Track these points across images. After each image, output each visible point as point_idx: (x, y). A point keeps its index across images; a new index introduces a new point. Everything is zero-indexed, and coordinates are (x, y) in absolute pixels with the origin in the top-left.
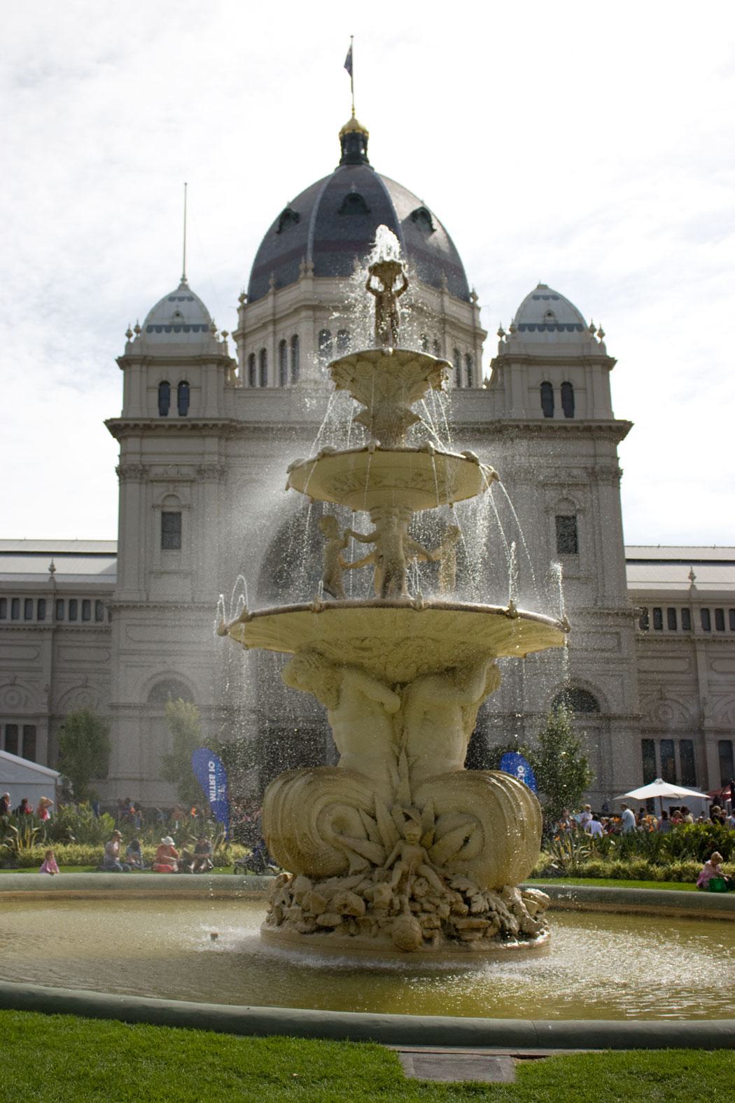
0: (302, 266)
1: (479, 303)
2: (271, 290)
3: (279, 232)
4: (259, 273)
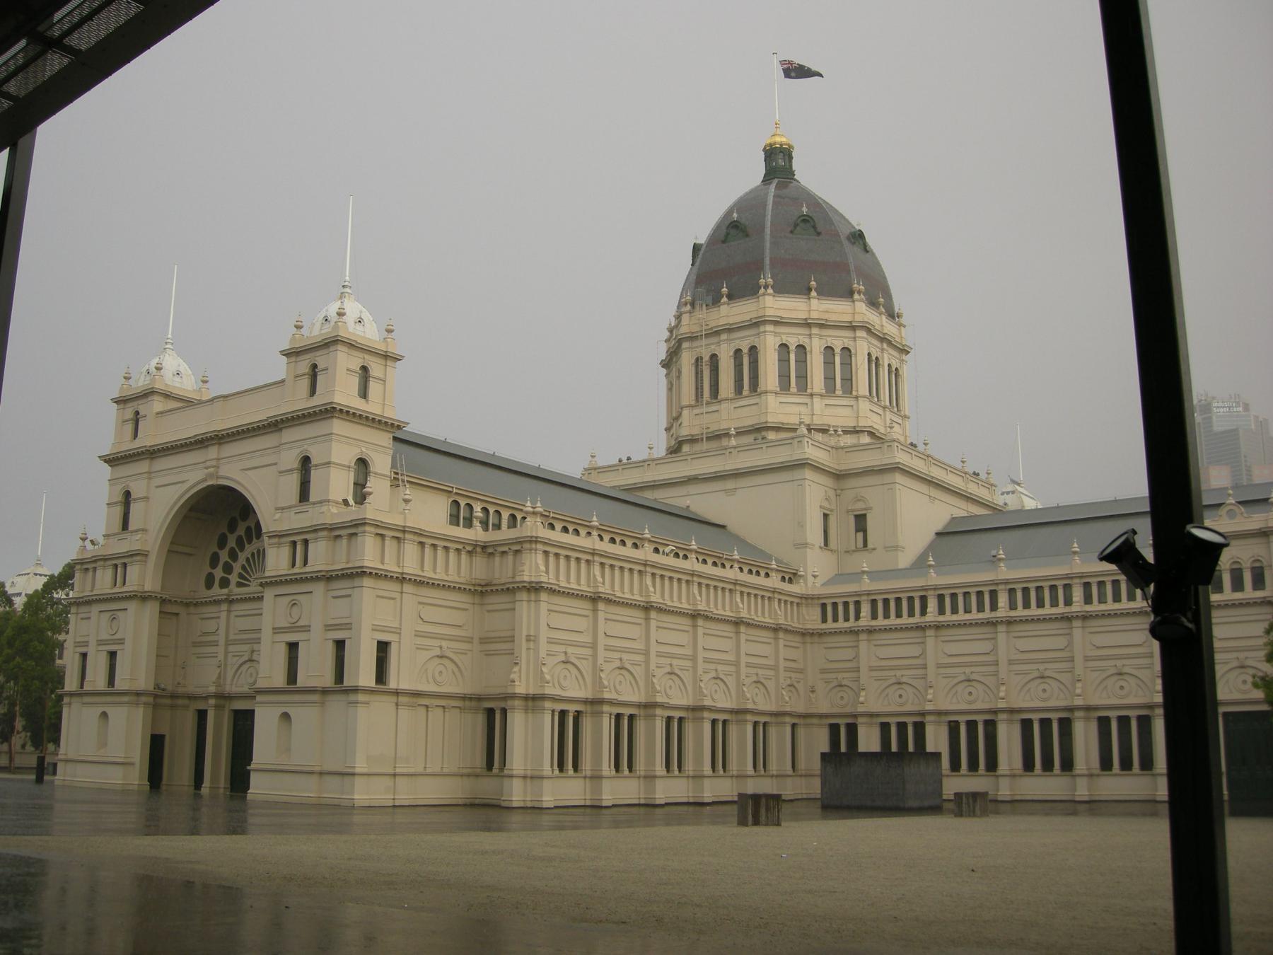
0: (762, 281)
1: (903, 321)
2: (725, 299)
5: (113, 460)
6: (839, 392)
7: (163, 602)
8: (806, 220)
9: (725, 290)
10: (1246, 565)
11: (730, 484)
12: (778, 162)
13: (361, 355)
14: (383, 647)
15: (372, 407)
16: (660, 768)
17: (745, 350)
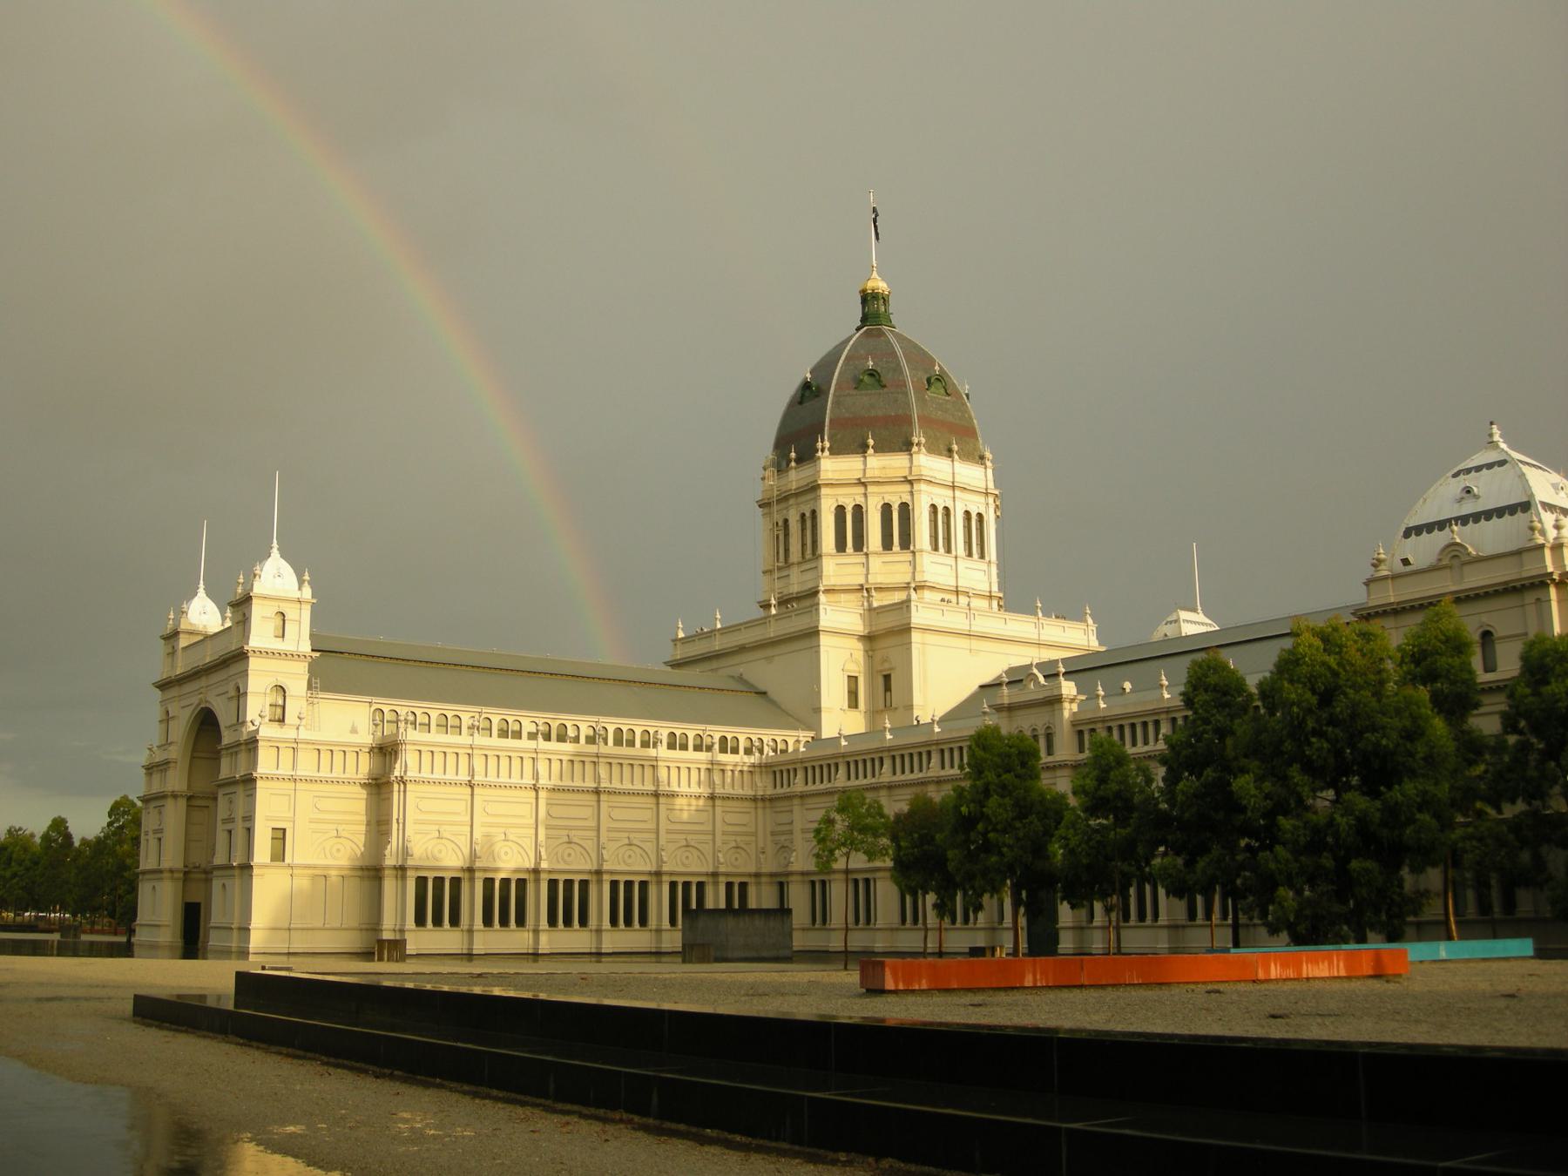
0: (819, 445)
3: (801, 403)
4: (782, 444)
5: (163, 686)
6: (896, 547)
7: (190, 798)
8: (872, 374)
9: (793, 455)
10: (1041, 731)
11: (769, 652)
12: (872, 308)
13: (276, 603)
14: (280, 836)
15: (287, 645)
16: (606, 923)
17: (808, 514)
